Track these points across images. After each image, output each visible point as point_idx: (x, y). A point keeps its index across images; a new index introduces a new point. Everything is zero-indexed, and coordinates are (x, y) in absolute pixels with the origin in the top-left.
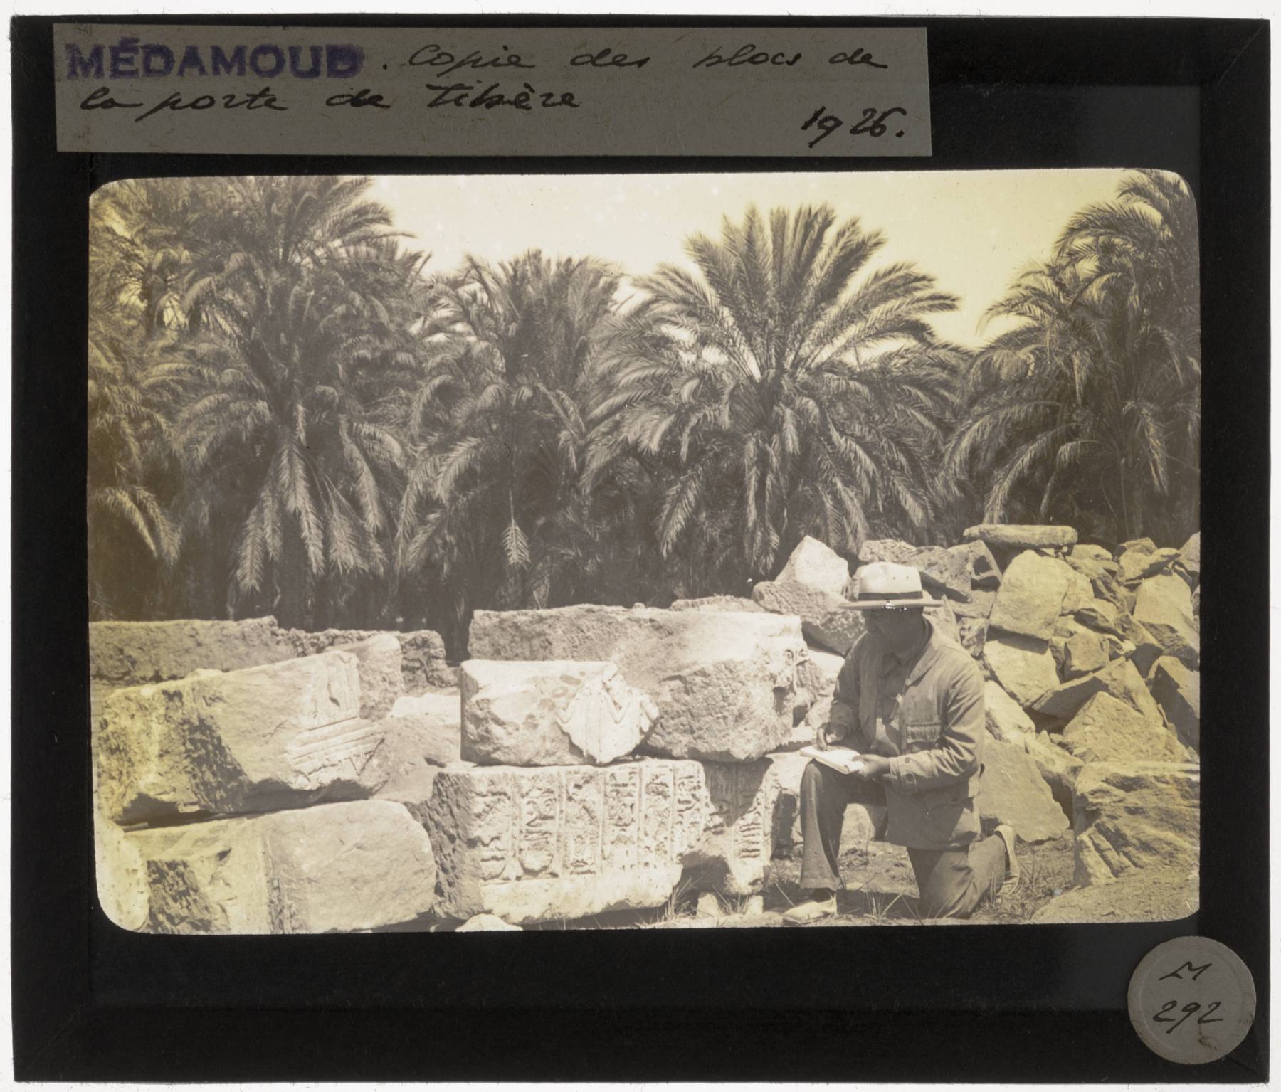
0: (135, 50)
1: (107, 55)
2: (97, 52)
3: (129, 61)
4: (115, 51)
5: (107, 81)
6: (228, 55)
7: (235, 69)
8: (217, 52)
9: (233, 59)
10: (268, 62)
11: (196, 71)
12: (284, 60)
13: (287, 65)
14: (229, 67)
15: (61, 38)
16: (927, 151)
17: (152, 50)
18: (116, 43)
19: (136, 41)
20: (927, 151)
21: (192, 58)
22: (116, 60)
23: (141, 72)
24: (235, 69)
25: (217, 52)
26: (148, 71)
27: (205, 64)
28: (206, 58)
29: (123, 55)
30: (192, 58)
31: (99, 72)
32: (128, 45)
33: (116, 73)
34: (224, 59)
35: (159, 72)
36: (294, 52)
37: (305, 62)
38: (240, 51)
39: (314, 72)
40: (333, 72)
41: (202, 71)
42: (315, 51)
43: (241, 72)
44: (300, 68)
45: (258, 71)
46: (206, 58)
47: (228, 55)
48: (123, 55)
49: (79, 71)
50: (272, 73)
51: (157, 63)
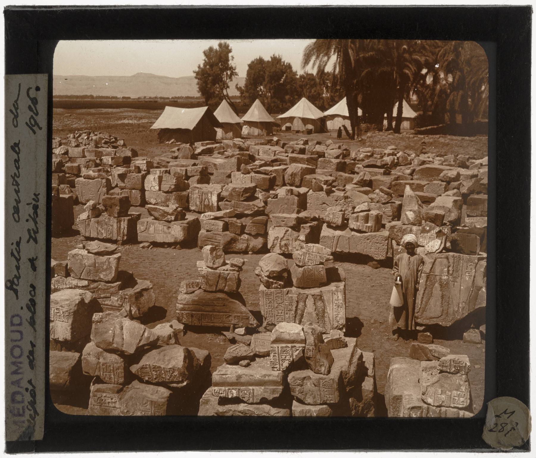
1: (17, 419)
3: (19, 409)
6: (17, 368)
8: (15, 372)
9: (17, 366)
14: (20, 368)
22: (20, 415)
28: (16, 377)
29: (16, 412)
34: (17, 370)
39: (21, 333)
42: (13, 331)
44: (19, 338)
50: (21, 350)
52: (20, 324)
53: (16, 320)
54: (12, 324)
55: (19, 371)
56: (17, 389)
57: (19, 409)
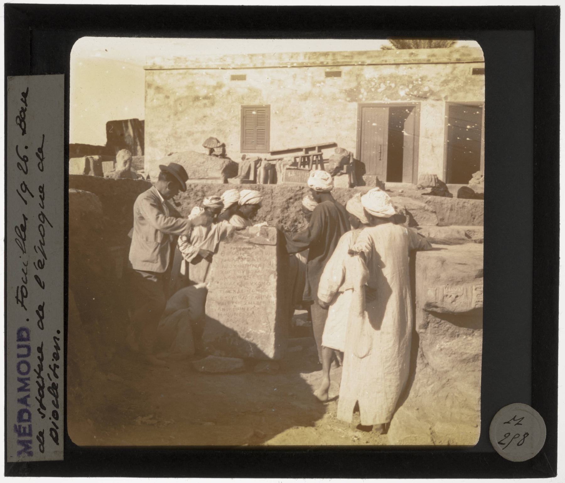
0: (20, 426)
2: (20, 442)
3: (24, 428)
4: (20, 435)
5: (34, 438)
6: (22, 385)
7: (27, 382)
8: (20, 390)
9: (23, 382)
10: (24, 368)
11: (28, 399)
12: (23, 360)
13: (27, 359)
14: (27, 385)
15: (15, 459)
16: (62, 76)
17: (20, 418)
18: (16, 434)
19: (15, 426)
20: (62, 76)
21: (23, 401)
22: (25, 434)
23: (29, 423)
24: (27, 382)
25: (20, 390)
26: (29, 420)
27: (25, 395)
28: (23, 394)
29: (22, 431)
30: (23, 401)
31: (30, 442)
32: (18, 430)
33: (30, 434)
35: (30, 415)
36: (19, 356)
37: (24, 351)
38: (20, 380)
39: (29, 348)
40: (28, 339)
41: (28, 396)
42: (19, 347)
43: (28, 379)
45: (27, 373)
46: (23, 394)
47: (22, 385)
48: (22, 431)
49: (30, 450)
51: (26, 416)
52: (28, 339)
53: (25, 334)
54: (20, 339)
55: (27, 388)
56: (23, 407)
57: (24, 428)
